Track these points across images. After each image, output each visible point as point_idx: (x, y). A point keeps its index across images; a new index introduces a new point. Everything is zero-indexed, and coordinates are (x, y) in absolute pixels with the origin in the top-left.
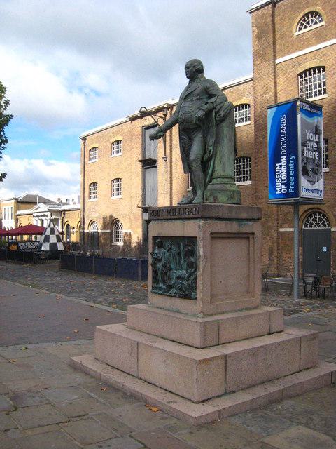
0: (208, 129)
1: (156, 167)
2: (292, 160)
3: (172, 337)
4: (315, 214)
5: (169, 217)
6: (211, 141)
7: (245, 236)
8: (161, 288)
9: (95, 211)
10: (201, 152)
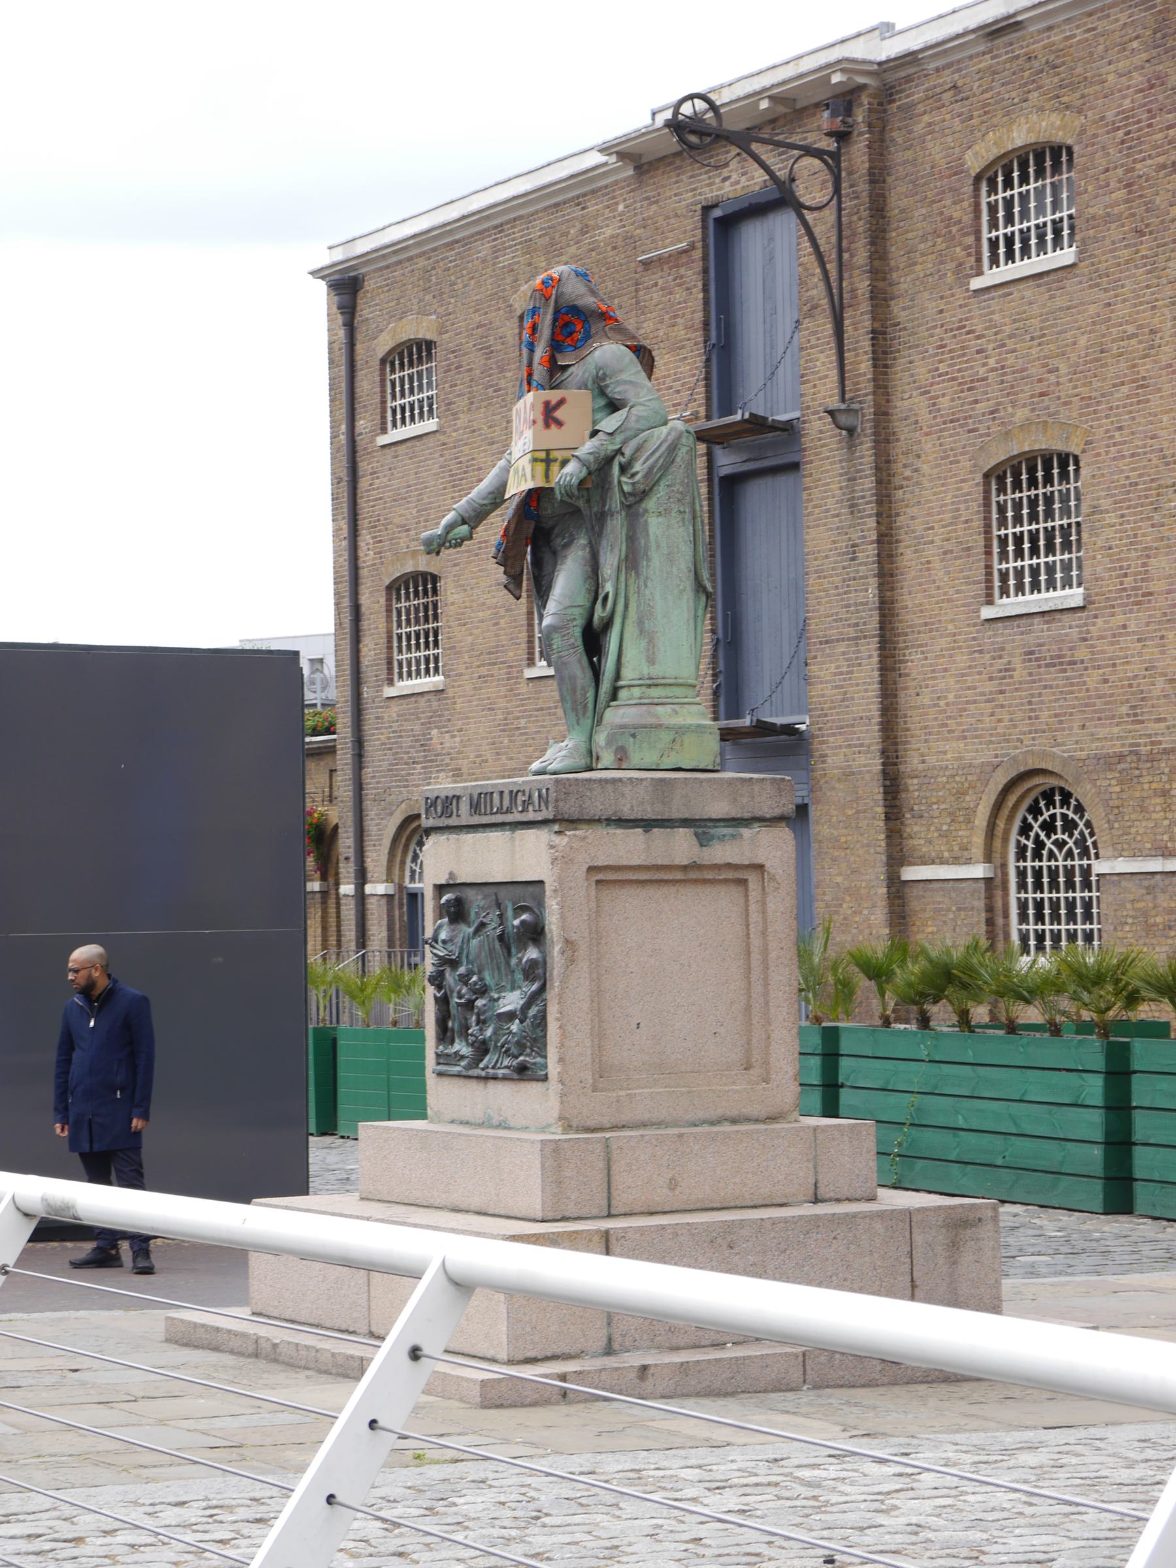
0: (602, 517)
1: (794, 467)
6: (609, 563)
7: (730, 875)
9: (432, 760)
10: (583, 599)
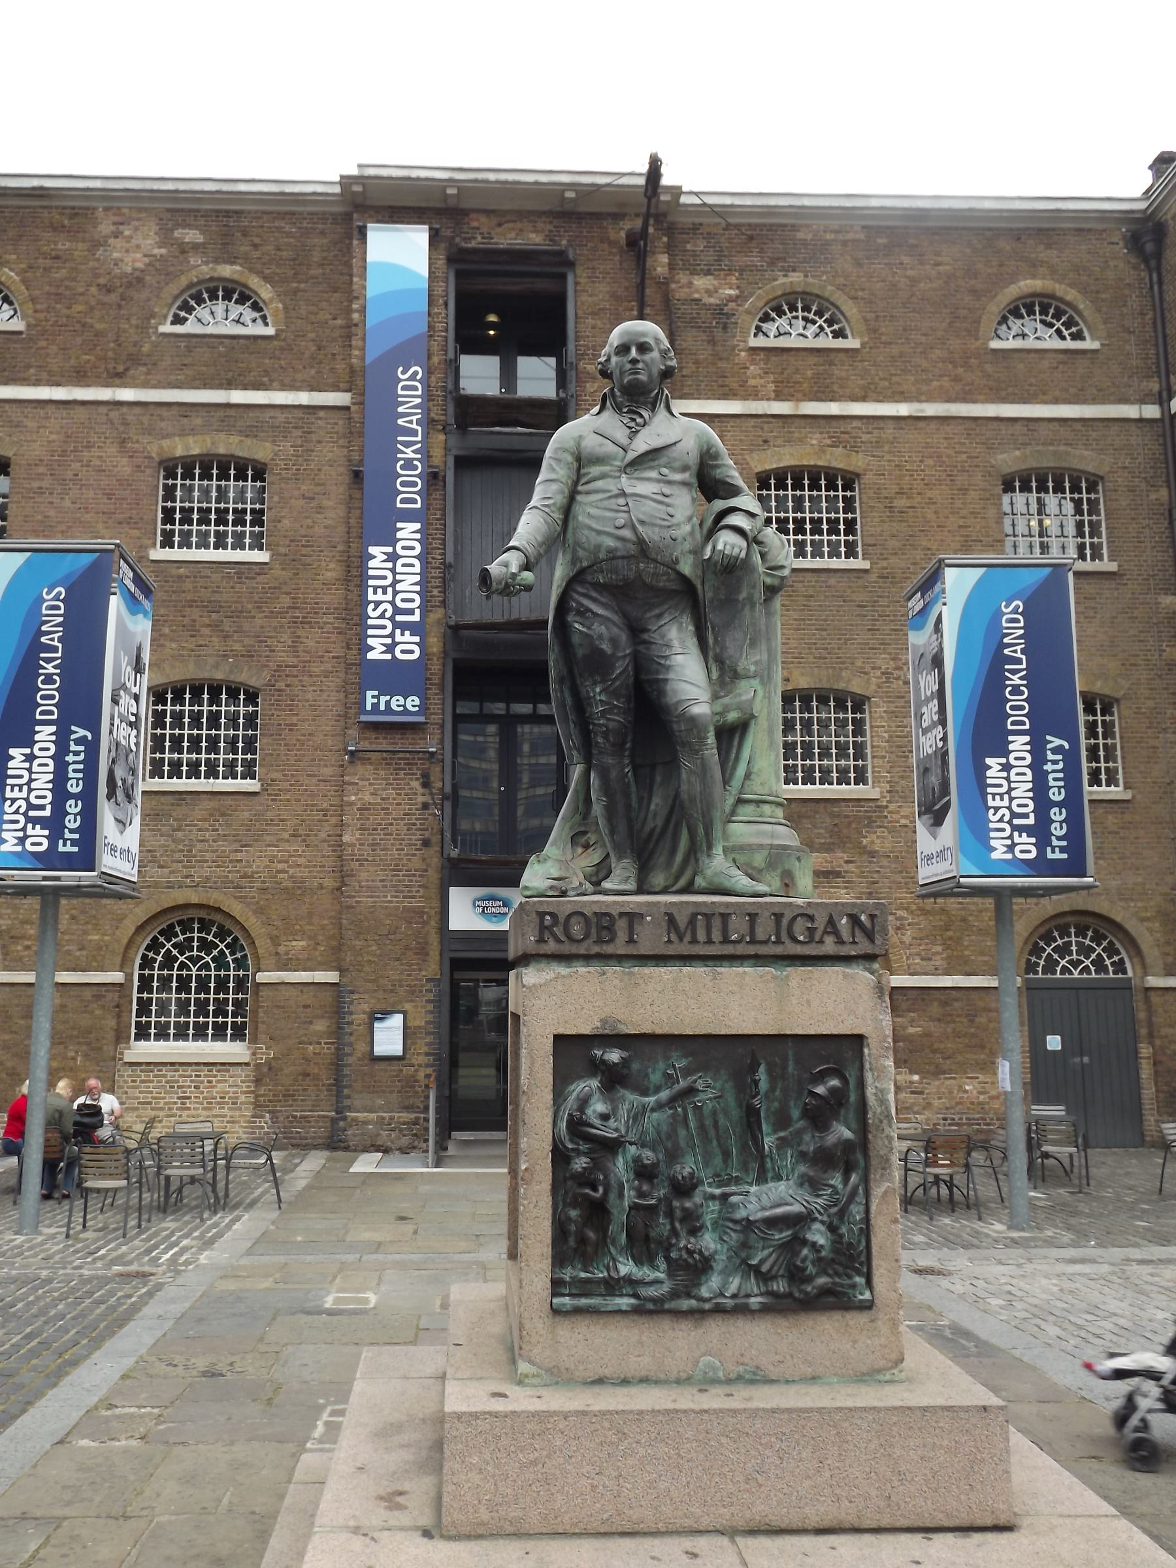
2: (78, 742)
5: (684, 948)
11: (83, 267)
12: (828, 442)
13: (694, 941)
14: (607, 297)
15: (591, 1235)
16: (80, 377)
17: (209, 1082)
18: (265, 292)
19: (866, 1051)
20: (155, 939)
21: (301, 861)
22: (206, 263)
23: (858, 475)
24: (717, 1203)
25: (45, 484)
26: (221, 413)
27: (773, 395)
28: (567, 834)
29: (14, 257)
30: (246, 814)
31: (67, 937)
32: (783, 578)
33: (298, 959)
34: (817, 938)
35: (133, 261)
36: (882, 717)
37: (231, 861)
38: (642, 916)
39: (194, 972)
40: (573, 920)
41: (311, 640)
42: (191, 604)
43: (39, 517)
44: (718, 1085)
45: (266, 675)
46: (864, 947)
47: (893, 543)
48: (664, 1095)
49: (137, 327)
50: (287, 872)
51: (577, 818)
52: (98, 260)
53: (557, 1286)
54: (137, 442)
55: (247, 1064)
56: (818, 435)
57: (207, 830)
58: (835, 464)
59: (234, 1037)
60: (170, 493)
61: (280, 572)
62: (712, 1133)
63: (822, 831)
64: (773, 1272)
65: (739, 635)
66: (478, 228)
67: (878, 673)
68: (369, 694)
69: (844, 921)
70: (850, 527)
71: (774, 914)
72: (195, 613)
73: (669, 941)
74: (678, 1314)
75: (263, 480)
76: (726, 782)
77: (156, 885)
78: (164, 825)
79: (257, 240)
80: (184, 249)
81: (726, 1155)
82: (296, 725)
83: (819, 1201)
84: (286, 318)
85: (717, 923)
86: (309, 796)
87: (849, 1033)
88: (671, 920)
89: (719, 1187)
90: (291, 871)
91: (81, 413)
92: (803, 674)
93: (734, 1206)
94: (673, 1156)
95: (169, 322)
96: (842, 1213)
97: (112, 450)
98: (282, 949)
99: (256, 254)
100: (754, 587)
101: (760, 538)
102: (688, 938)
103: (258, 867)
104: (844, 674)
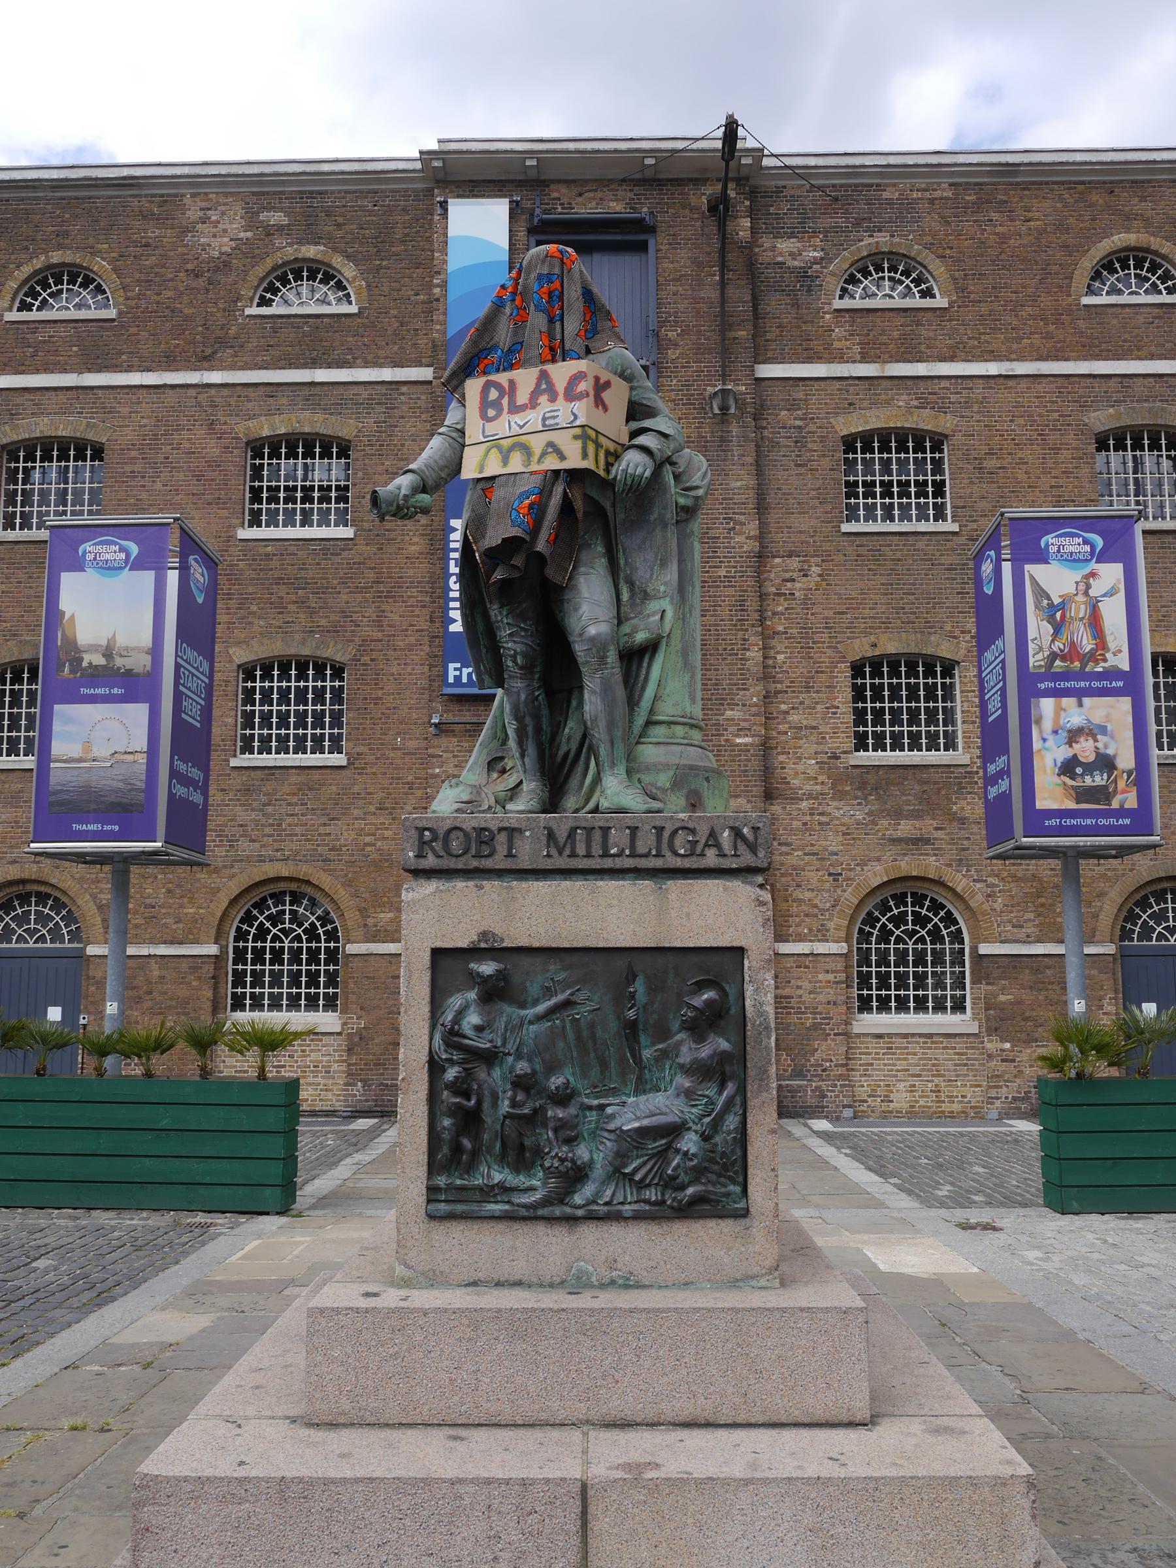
3: (686, 1413)
4: (278, 898)
8: (490, 1192)
11: (172, 253)
12: (916, 403)
13: (573, 855)
14: (688, 263)
15: (467, 1143)
16: (170, 362)
17: (303, 1051)
18: (348, 271)
19: (746, 962)
20: (248, 912)
21: (388, 833)
22: (291, 245)
23: (946, 436)
24: (594, 1113)
25: (136, 468)
26: (306, 391)
27: (858, 357)
28: (484, 759)
29: (106, 246)
30: (334, 788)
31: (164, 911)
32: (697, 498)
33: (386, 931)
34: (698, 851)
35: (221, 245)
36: (971, 682)
37: (319, 835)
38: (520, 831)
39: (286, 945)
40: (453, 835)
41: (395, 614)
42: (279, 581)
43: (132, 501)
44: (596, 998)
45: (352, 650)
46: (747, 859)
47: (983, 505)
48: (541, 1008)
49: (224, 310)
50: (374, 845)
51: (495, 744)
52: (187, 245)
53: (432, 1192)
54: (225, 423)
55: (339, 1034)
56: (905, 397)
57: (296, 804)
58: (922, 426)
59: (326, 1008)
60: (257, 473)
61: (364, 548)
62: (590, 1044)
63: (910, 798)
64: (647, 1181)
65: (650, 556)
66: (559, 199)
67: (968, 637)
68: (451, 666)
69: (726, 834)
70: (939, 490)
71: (654, 827)
72: (282, 591)
73: (549, 856)
74: (550, 1220)
75: (348, 457)
76: (632, 702)
77: (248, 859)
78: (255, 800)
79: (340, 220)
80: (270, 231)
81: (604, 1065)
82: (381, 699)
83: (694, 1110)
84: (369, 295)
85: (597, 836)
86: (395, 769)
87: (729, 945)
88: (551, 835)
89: (597, 1098)
90: (379, 844)
91: (171, 397)
92: (890, 639)
93: (612, 1117)
94: (552, 1068)
95: (255, 304)
96: (716, 1124)
97: (201, 432)
98: (370, 921)
99: (339, 234)
100: (665, 508)
101: (674, 459)
102: (567, 851)
103: (346, 840)
104: (933, 638)
